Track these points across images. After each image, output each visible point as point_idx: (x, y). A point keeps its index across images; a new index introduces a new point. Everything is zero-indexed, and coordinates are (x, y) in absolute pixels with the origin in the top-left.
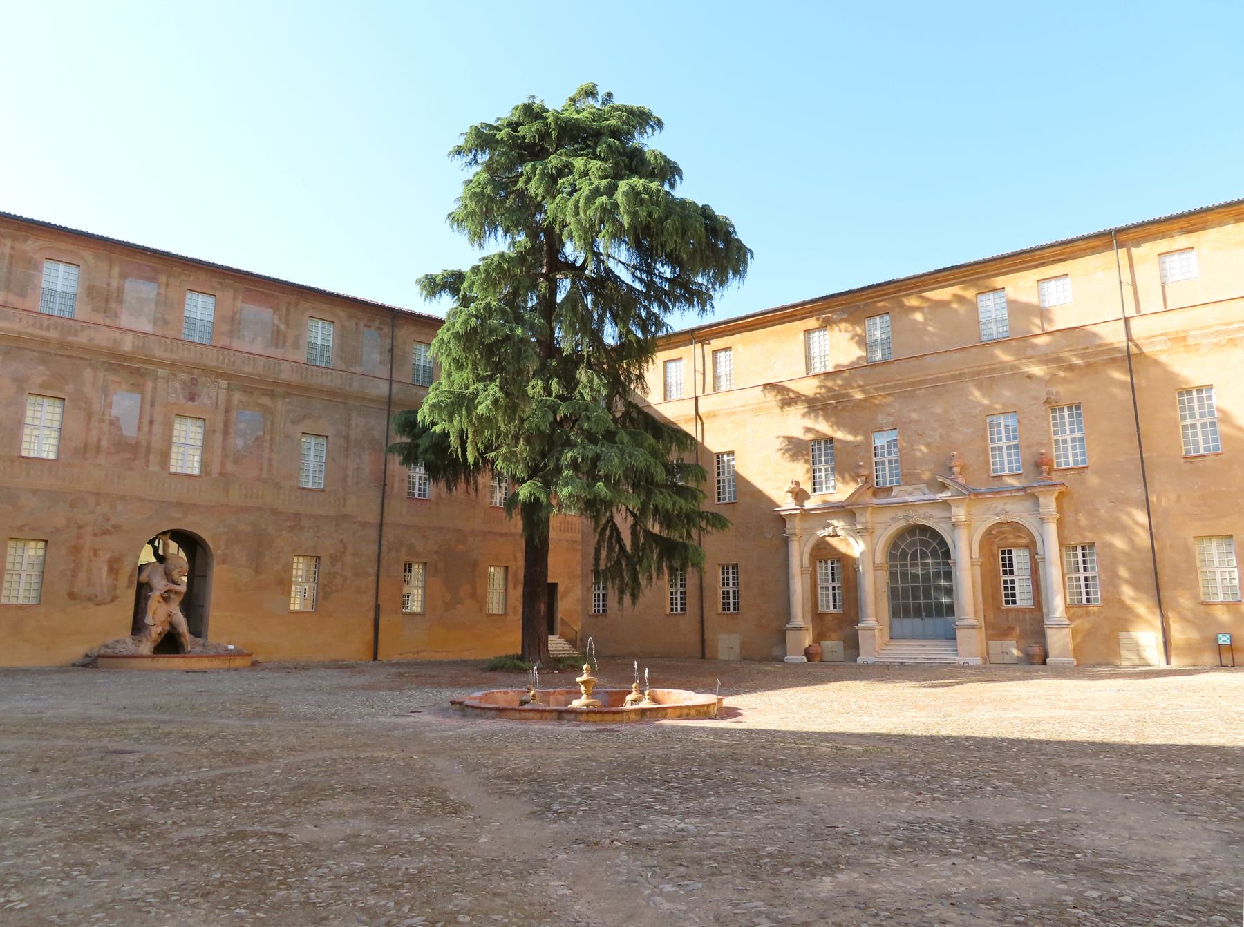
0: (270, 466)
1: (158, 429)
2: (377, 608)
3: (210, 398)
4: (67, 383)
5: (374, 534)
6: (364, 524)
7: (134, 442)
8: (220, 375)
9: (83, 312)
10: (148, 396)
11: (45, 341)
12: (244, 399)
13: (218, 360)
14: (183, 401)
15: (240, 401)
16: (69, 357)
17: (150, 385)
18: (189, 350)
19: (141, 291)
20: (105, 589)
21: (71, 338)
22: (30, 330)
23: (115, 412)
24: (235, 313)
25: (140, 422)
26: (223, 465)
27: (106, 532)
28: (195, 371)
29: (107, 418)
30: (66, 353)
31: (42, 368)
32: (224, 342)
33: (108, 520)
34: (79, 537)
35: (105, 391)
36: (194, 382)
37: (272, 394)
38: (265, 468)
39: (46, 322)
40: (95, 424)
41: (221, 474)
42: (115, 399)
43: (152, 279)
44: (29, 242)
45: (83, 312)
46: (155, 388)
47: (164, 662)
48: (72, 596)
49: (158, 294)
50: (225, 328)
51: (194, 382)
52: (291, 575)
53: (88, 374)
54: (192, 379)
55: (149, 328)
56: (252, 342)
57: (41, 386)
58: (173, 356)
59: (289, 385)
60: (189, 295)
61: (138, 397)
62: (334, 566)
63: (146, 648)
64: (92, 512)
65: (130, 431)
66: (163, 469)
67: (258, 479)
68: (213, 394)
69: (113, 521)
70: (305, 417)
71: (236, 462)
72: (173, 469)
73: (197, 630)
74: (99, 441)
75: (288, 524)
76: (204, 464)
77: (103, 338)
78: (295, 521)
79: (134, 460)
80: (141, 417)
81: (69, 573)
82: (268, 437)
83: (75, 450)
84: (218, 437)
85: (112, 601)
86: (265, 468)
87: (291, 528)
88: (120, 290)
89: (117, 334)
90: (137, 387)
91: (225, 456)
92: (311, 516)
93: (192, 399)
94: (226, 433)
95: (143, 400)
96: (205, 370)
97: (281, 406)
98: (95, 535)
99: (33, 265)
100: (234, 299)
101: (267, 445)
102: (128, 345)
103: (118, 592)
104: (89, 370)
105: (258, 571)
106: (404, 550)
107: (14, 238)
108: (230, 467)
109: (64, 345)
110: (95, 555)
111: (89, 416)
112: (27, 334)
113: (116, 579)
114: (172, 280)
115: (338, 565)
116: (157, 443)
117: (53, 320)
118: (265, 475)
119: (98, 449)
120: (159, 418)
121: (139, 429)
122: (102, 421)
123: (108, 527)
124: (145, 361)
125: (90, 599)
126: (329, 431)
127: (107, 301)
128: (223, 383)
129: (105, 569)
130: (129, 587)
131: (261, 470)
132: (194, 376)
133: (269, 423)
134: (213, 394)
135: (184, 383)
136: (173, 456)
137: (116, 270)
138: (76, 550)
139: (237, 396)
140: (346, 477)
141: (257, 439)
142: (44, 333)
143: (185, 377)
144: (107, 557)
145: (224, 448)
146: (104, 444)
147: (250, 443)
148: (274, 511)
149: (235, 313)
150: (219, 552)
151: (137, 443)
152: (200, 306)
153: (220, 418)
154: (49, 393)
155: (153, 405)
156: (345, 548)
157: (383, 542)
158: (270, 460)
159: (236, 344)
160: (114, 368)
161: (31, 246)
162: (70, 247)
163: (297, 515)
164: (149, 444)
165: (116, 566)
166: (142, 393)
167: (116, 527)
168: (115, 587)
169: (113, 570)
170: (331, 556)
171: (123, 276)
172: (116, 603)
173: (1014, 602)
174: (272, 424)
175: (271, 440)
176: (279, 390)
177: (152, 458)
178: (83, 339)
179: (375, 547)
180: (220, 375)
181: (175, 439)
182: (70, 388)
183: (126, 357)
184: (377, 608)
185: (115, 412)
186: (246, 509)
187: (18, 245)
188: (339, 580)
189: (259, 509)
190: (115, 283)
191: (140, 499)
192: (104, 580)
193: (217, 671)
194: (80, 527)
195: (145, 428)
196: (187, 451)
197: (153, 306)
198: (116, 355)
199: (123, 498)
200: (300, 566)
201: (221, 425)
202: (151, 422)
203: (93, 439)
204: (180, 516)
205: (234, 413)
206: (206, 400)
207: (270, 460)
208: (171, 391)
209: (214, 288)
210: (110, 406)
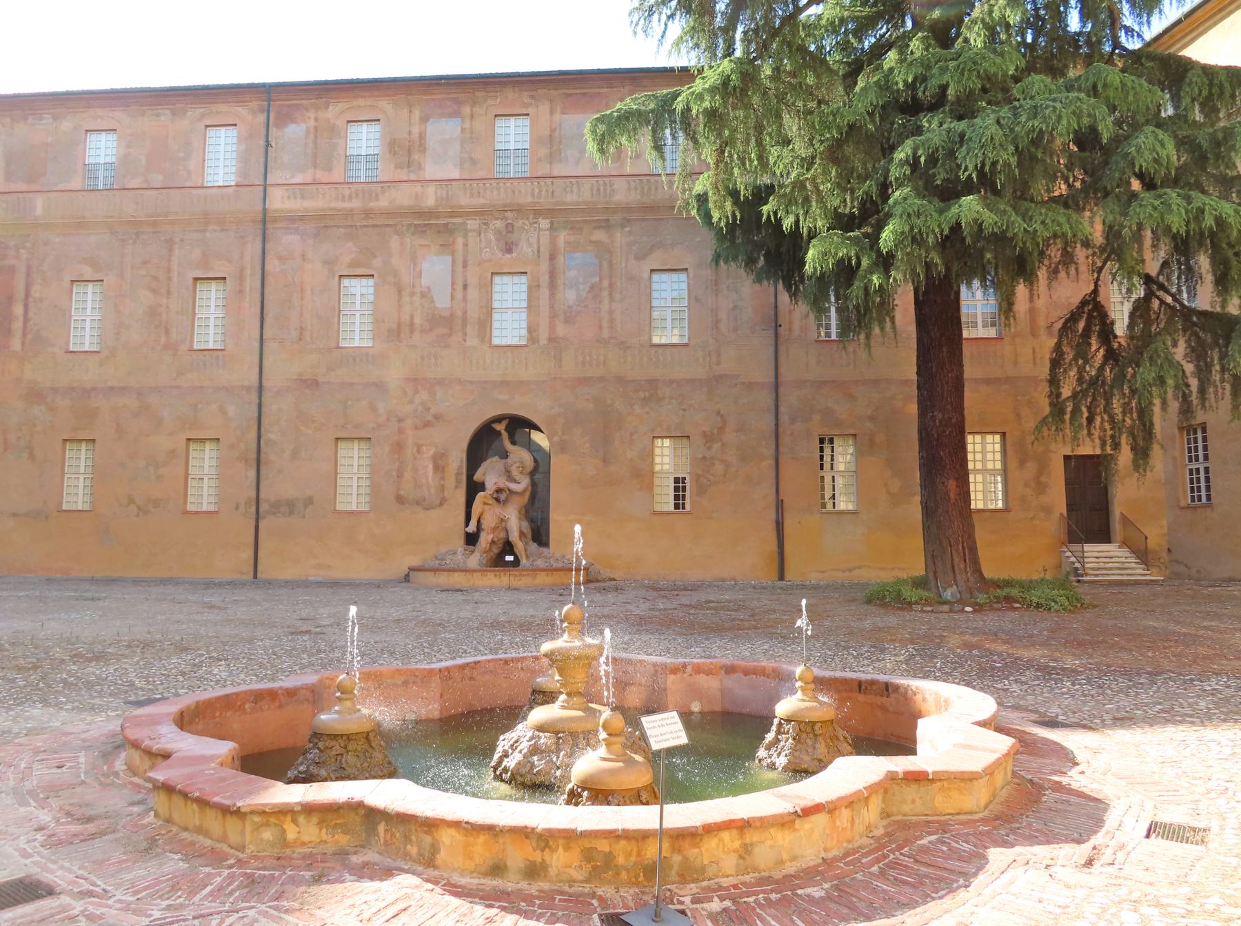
0: (612, 321)
1: (473, 293)
2: (780, 506)
3: (530, 245)
4: (375, 257)
5: (766, 398)
6: (750, 386)
7: (447, 314)
8: (538, 213)
9: (385, 172)
11: (349, 214)
12: (572, 238)
13: (533, 195)
14: (499, 254)
15: (567, 243)
16: (374, 226)
17: (460, 241)
18: (499, 189)
19: (444, 131)
20: (433, 491)
21: (373, 204)
22: (333, 205)
24: (553, 131)
25: (453, 289)
26: (552, 327)
27: (427, 425)
28: (509, 214)
29: (418, 290)
30: (370, 222)
31: (350, 244)
32: (543, 170)
33: (428, 409)
34: (401, 431)
35: (414, 259)
36: (510, 228)
37: (606, 225)
38: (605, 324)
39: (347, 192)
40: (406, 299)
41: (550, 340)
42: (425, 266)
43: (455, 114)
44: (331, 108)
45: (385, 172)
46: (466, 245)
47: (495, 579)
48: (400, 500)
49: (463, 130)
50: (543, 152)
51: (510, 228)
52: (652, 463)
53: (394, 242)
54: (507, 225)
55: (455, 174)
56: (577, 163)
57: (351, 265)
58: (482, 201)
59: (628, 209)
60: (500, 123)
61: (449, 259)
62: (709, 448)
64: (411, 402)
65: (442, 301)
66: (483, 341)
67: (598, 341)
68: (534, 238)
69: (433, 411)
70: (653, 248)
71: (568, 320)
72: (496, 342)
74: (412, 317)
75: (642, 395)
76: (531, 329)
77: (403, 197)
78: (651, 391)
79: (450, 335)
80: (453, 284)
81: (394, 473)
82: (606, 284)
83: (393, 332)
84: (545, 292)
85: (441, 504)
86: (605, 324)
87: (645, 401)
88: (422, 136)
89: (418, 188)
90: (447, 247)
91: (553, 316)
92: (671, 382)
94: (553, 285)
96: (519, 210)
97: (620, 238)
98: (416, 428)
99: (334, 132)
100: (552, 112)
101: (605, 294)
102: (430, 198)
103: (446, 493)
104: (395, 237)
105: (605, 461)
106: (817, 418)
107: (317, 108)
108: (561, 330)
109: (368, 213)
110: (418, 452)
111: (400, 292)
112: (331, 209)
114: (477, 109)
116: (474, 313)
117: (354, 187)
118: (606, 334)
119: (412, 325)
120: (473, 280)
121: (452, 298)
122: (412, 294)
123: (430, 418)
124: (452, 214)
126: (688, 261)
127: (410, 152)
128: (544, 223)
130: (456, 487)
131: (600, 327)
132: (508, 219)
133: (605, 264)
134: (534, 238)
135: (498, 232)
136: (496, 325)
137: (417, 114)
138: (399, 447)
139: (562, 237)
140: (717, 322)
141: (592, 287)
142: (347, 205)
143: (499, 224)
144: (431, 452)
145: (552, 307)
146: (417, 320)
147: (584, 294)
148: (621, 380)
151: (452, 315)
152: (513, 134)
153: (544, 267)
154: (359, 272)
155: (465, 265)
156: (725, 422)
157: (782, 409)
158: (611, 312)
159: (558, 170)
160: (420, 230)
161: (334, 111)
162: (368, 102)
163: (653, 383)
164: (465, 313)
165: (441, 463)
166: (453, 253)
167: (437, 417)
169: (439, 468)
170: (705, 435)
171: (424, 120)
172: (445, 507)
174: (611, 264)
175: (611, 286)
176: (616, 218)
177: (469, 330)
178: (383, 203)
179: (769, 419)
180: (538, 213)
181: (495, 304)
182: (377, 262)
183: (431, 213)
184: (780, 506)
185: (425, 281)
186: (585, 381)
187: (323, 115)
188: (719, 468)
189: (601, 379)
190: (416, 130)
191: (460, 382)
193: (494, 590)
194: (400, 420)
195: (459, 295)
197: (458, 147)
198: (421, 214)
199: (441, 382)
200: (666, 452)
201: (547, 277)
202: (465, 287)
203: (406, 318)
204: (506, 397)
205: (560, 259)
206: (525, 248)
207: (611, 312)
208: (481, 244)
209: (526, 105)
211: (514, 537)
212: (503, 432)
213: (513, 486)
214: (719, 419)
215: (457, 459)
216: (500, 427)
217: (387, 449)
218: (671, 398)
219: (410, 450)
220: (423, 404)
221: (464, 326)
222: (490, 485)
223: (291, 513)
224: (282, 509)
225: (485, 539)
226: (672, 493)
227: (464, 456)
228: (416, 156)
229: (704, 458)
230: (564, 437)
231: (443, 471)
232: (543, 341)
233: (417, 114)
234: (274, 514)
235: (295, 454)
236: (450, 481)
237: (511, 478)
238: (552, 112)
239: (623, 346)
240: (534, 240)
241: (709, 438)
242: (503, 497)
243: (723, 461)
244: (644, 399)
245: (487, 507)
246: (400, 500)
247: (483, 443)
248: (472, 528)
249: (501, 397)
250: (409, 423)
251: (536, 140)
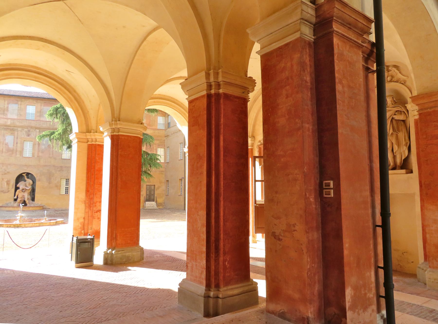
8: (36, 128)
10: (16, 136)
17: (16, 133)
23: (6, 141)
24: (41, 110)
26: (38, 154)
27: (5, 174)
35: (4, 136)
36: (29, 131)
41: (38, 156)
43: (17, 103)
46: (18, 134)
50: (38, 114)
51: (29, 131)
55: (16, 117)
61: (13, 137)
65: (11, 146)
69: (7, 171)
71: (42, 152)
73: (33, 199)
74: (3, 149)
76: (33, 154)
85: (8, 192)
87: (59, 171)
88: (7, 108)
89: (6, 120)
90: (12, 134)
91: (39, 151)
93: (29, 136)
95: (14, 137)
96: (31, 127)
100: (41, 106)
102: (9, 122)
105: (49, 183)
108: (40, 154)
114: (22, 103)
116: (19, 149)
118: (51, 156)
120: (19, 142)
122: (3, 144)
124: (14, 127)
127: (4, 111)
128: (38, 131)
129: (6, 183)
131: (50, 154)
132: (29, 129)
135: (26, 132)
137: (6, 102)
143: (26, 130)
145: (38, 149)
146: (4, 150)
148: (54, 166)
149: (41, 110)
152: (31, 109)
155: (17, 138)
163: (61, 167)
166: (14, 135)
167: (8, 172)
168: (9, 188)
171: (8, 104)
177: (17, 153)
180: (36, 128)
183: (9, 126)
185: (6, 141)
190: (6, 106)
195: (15, 145)
196: (28, 150)
198: (6, 126)
199: (10, 164)
202: (17, 143)
210: (5, 140)
211: (26, 200)
215: (13, 182)
216: (24, 175)
221: (16, 152)
222: (21, 188)
225: (19, 200)
228: (6, 112)
232: (36, 156)
233: (6, 102)
237: (26, 186)
238: (41, 106)
239: (55, 159)
240: (35, 134)
242: (24, 191)
247: (20, 178)
248: (16, 197)
251: (37, 112)
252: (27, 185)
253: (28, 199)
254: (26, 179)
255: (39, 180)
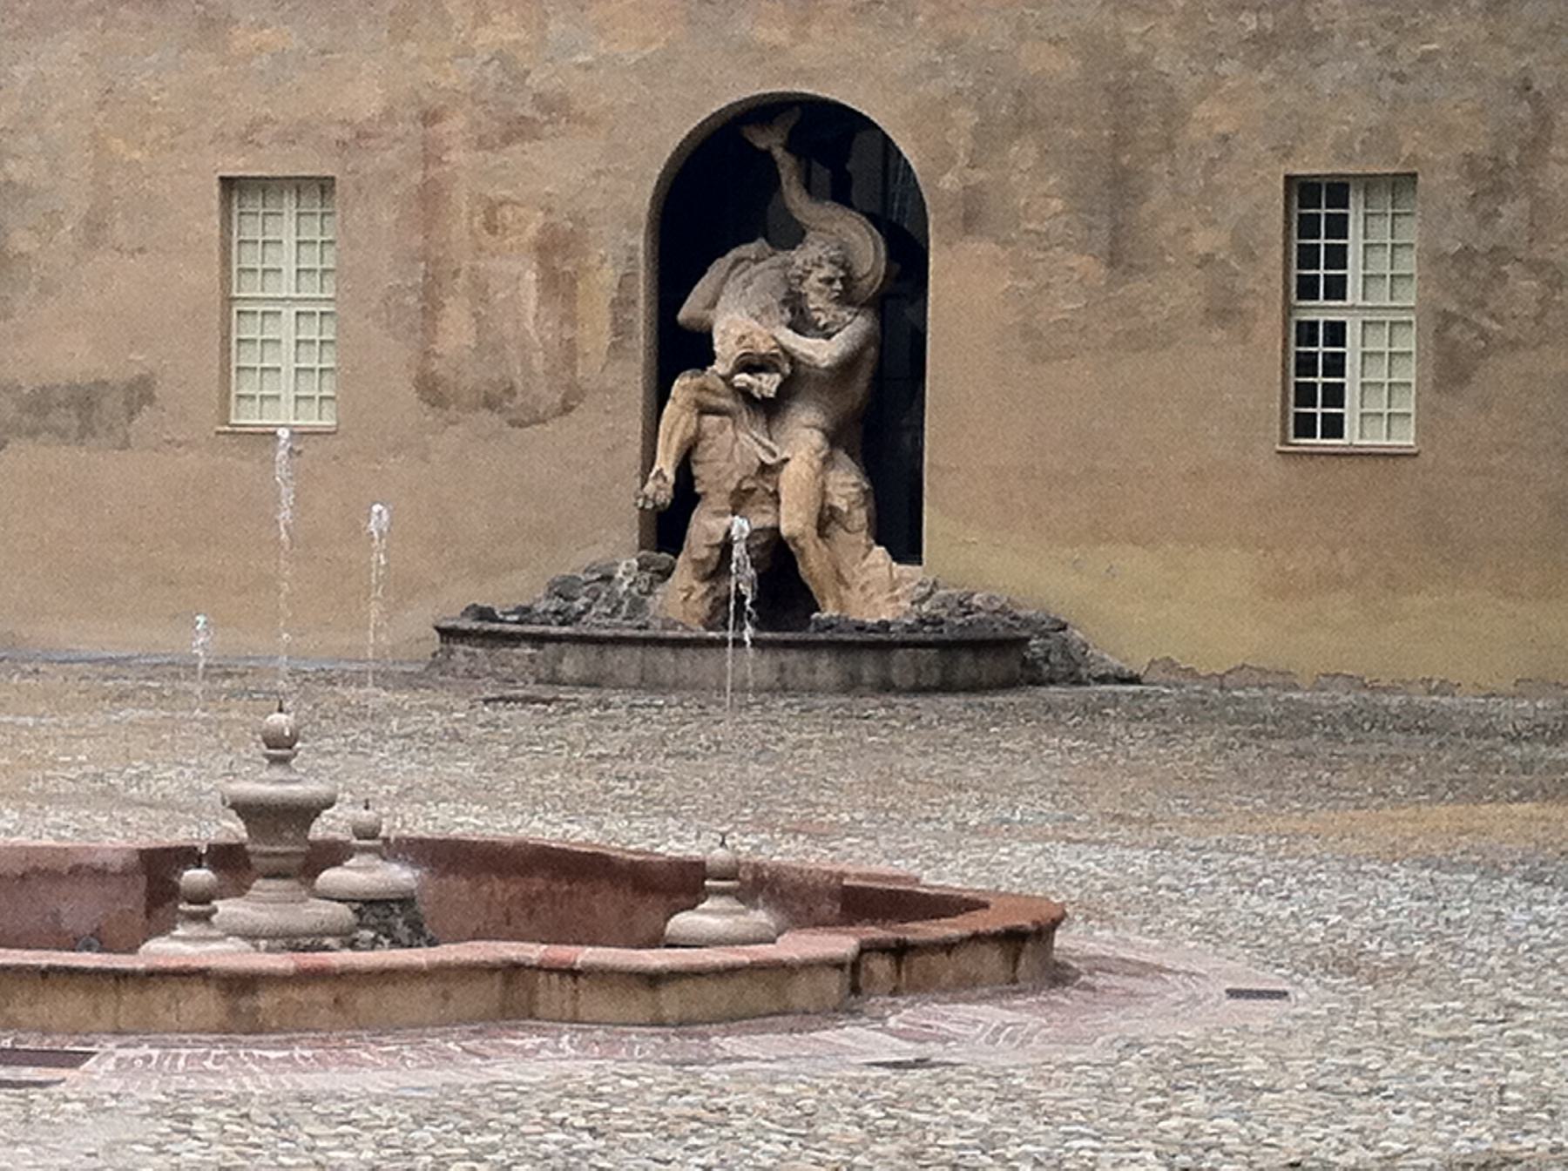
20: (538, 362)
27: (517, 130)
62: (1489, 218)
63: (680, 599)
64: (465, 52)
73: (899, 529)
85: (566, 409)
87: (1263, 45)
98: (481, 143)
113: (570, 319)
115: (1511, 213)
125: (490, 403)
129: (531, 276)
144: (532, 230)
150: (949, 182)
167: (555, 106)
168: (570, 352)
169: (559, 285)
173: (1334, 427)
192: (529, 324)
212: (778, 153)
213: (804, 346)
214: (1524, 111)
215: (620, 249)
216: (770, 141)
217: (387, 218)
218: (1356, 34)
219: (462, 221)
220: (503, 58)
222: (726, 348)
223: (86, 431)
224: (57, 418)
226: (1351, 380)
227: (639, 241)
229: (1467, 255)
230: (981, 175)
231: (570, 298)
234: (33, 433)
235: (95, 229)
236: (596, 333)
237: (802, 323)
241: (1489, 181)
243: (1536, 267)
244: (1257, 38)
245: (711, 421)
246: (432, 391)
247: (718, 193)
249: (762, 34)
250: (456, 123)
252: (818, 304)
253: (826, 520)
254: (795, 198)
255: (970, 220)
